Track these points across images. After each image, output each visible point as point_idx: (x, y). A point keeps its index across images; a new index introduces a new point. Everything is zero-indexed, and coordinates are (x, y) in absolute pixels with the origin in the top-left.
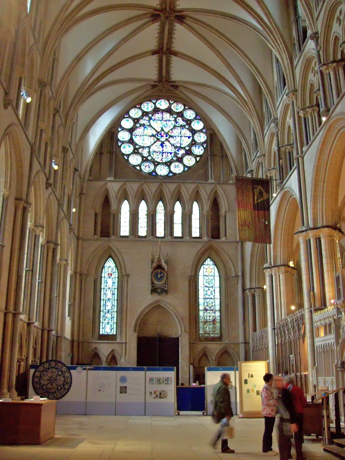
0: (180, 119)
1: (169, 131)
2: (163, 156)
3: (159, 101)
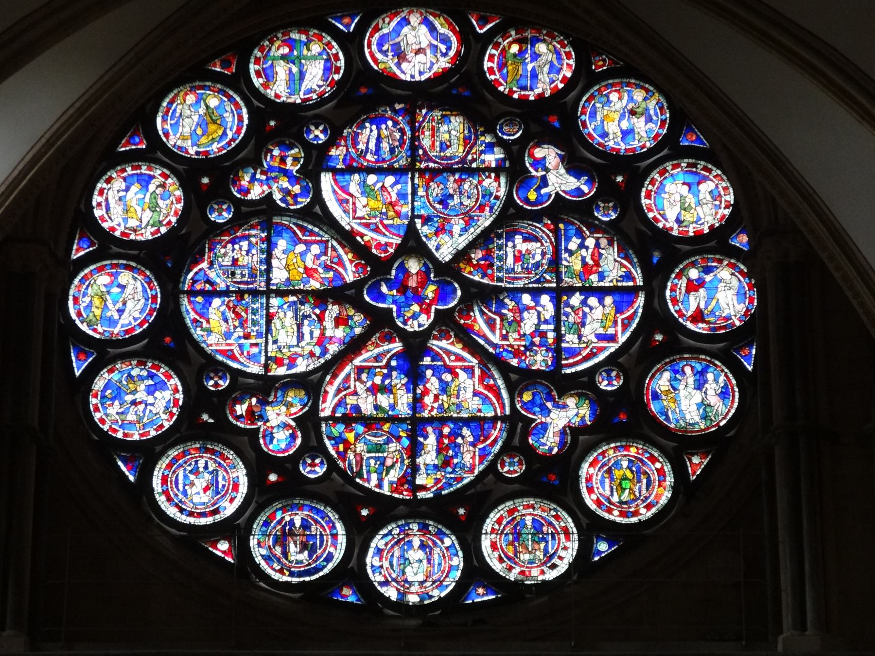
0: (549, 154)
1: (462, 255)
2: (414, 450)
3: (388, 26)
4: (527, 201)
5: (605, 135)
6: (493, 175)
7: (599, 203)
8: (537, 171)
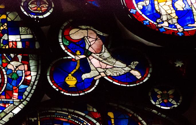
4: (67, 88)
5: (156, 15)
6: (20, 57)
7: (156, 90)
8: (75, 54)
